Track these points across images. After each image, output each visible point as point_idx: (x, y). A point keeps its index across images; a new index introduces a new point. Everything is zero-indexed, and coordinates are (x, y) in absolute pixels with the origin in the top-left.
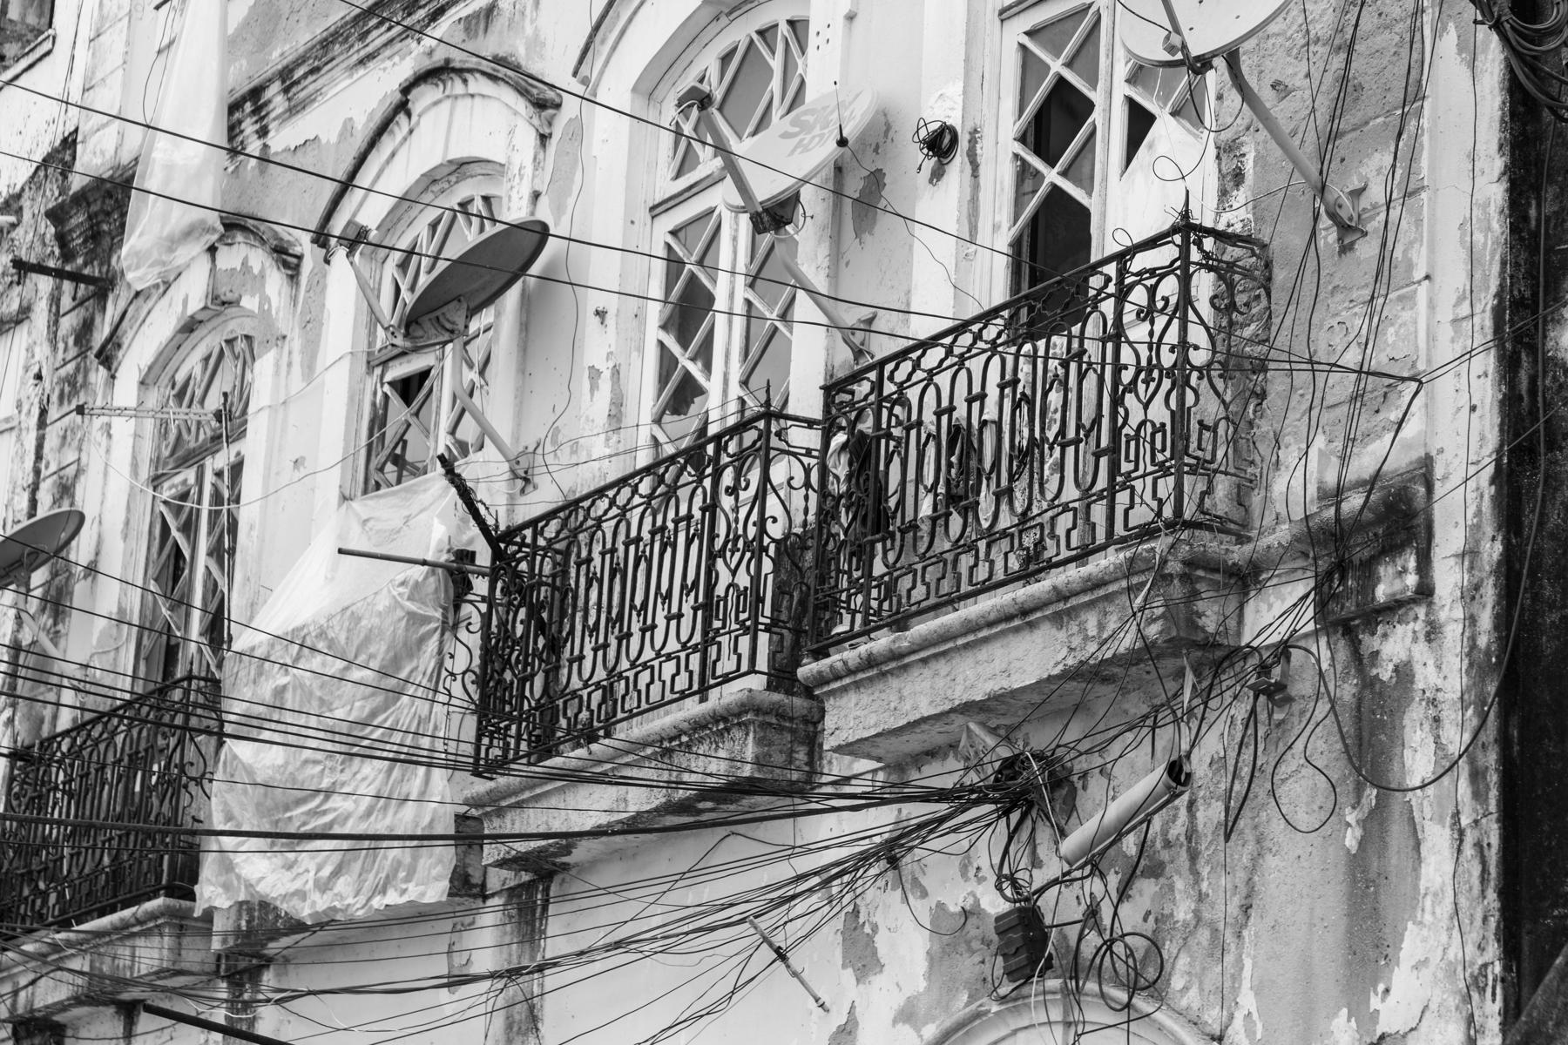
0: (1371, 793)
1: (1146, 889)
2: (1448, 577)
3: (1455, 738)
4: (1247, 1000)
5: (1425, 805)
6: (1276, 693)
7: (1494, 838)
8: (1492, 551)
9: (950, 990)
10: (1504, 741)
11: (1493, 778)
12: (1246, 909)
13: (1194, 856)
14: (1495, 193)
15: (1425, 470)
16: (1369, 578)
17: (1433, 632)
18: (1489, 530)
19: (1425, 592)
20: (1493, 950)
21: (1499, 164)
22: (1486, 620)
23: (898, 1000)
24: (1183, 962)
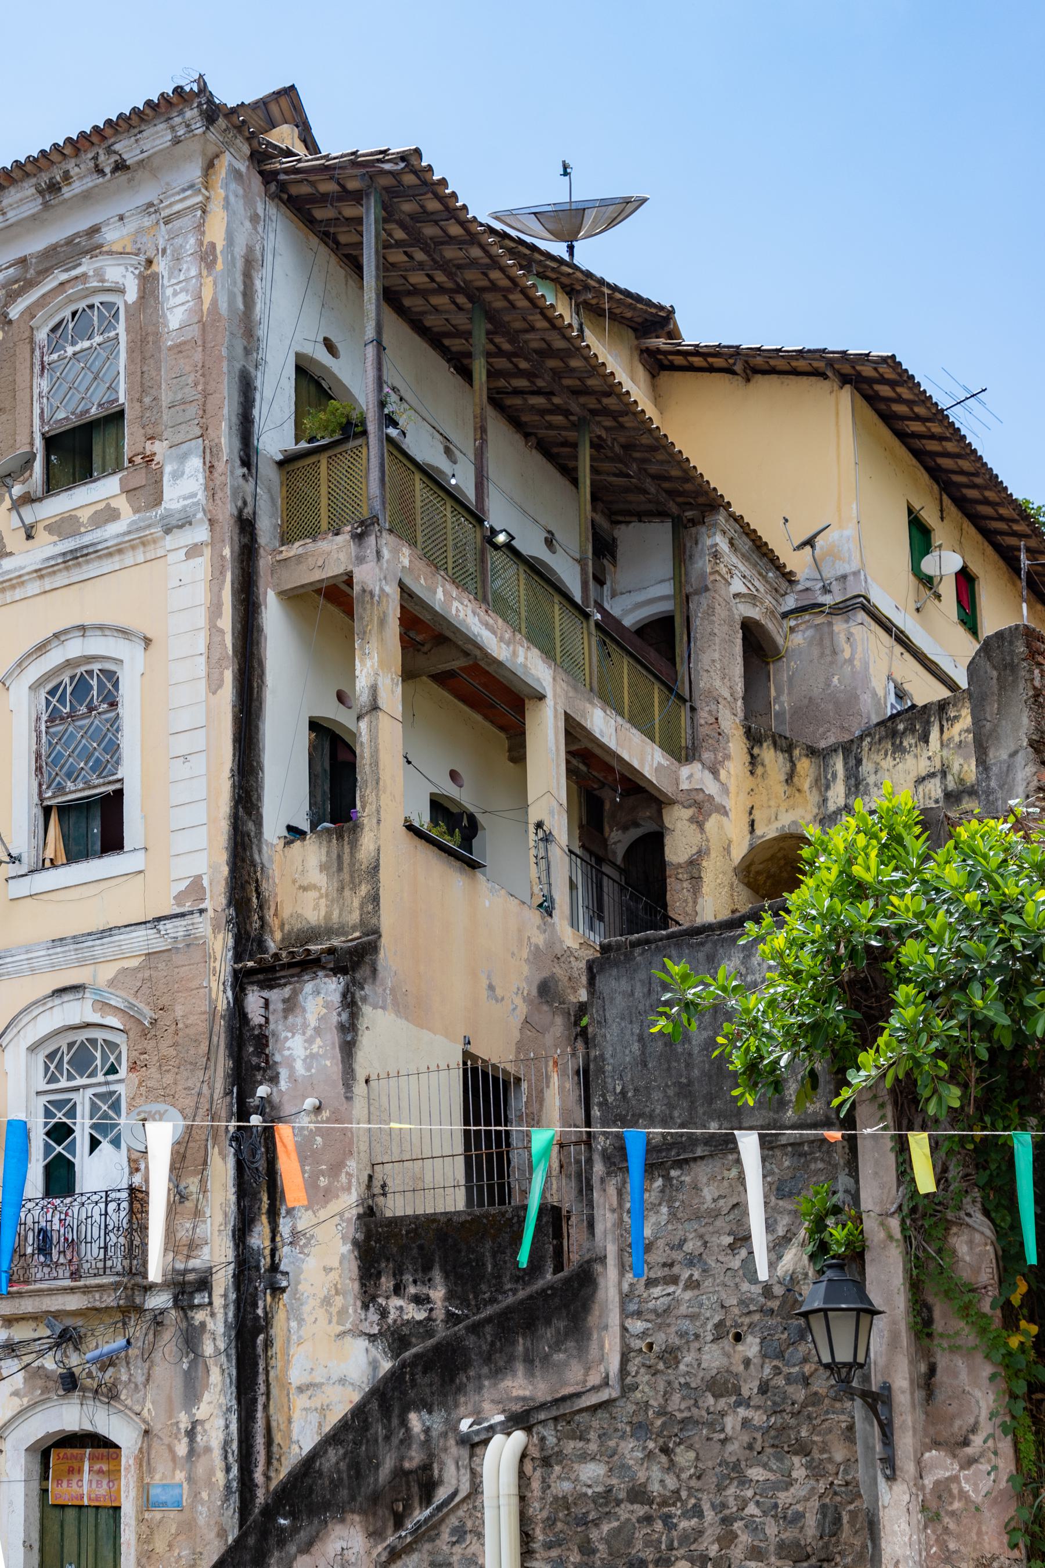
0: (192, 1355)
1: (111, 1370)
2: (218, 1302)
3: (222, 1346)
4: (149, 1405)
5: (210, 1362)
6: (159, 1324)
7: (234, 1372)
8: (233, 1296)
9: (33, 1388)
10: (237, 1347)
11: (234, 1357)
12: (148, 1380)
13: (128, 1363)
14: (233, 1198)
15: (209, 1271)
16: (192, 1298)
17: (213, 1315)
18: (231, 1290)
19: (210, 1304)
20: (234, 1402)
21: (233, 1190)
22: (231, 1314)
23: (12, 1389)
24: (124, 1392)
